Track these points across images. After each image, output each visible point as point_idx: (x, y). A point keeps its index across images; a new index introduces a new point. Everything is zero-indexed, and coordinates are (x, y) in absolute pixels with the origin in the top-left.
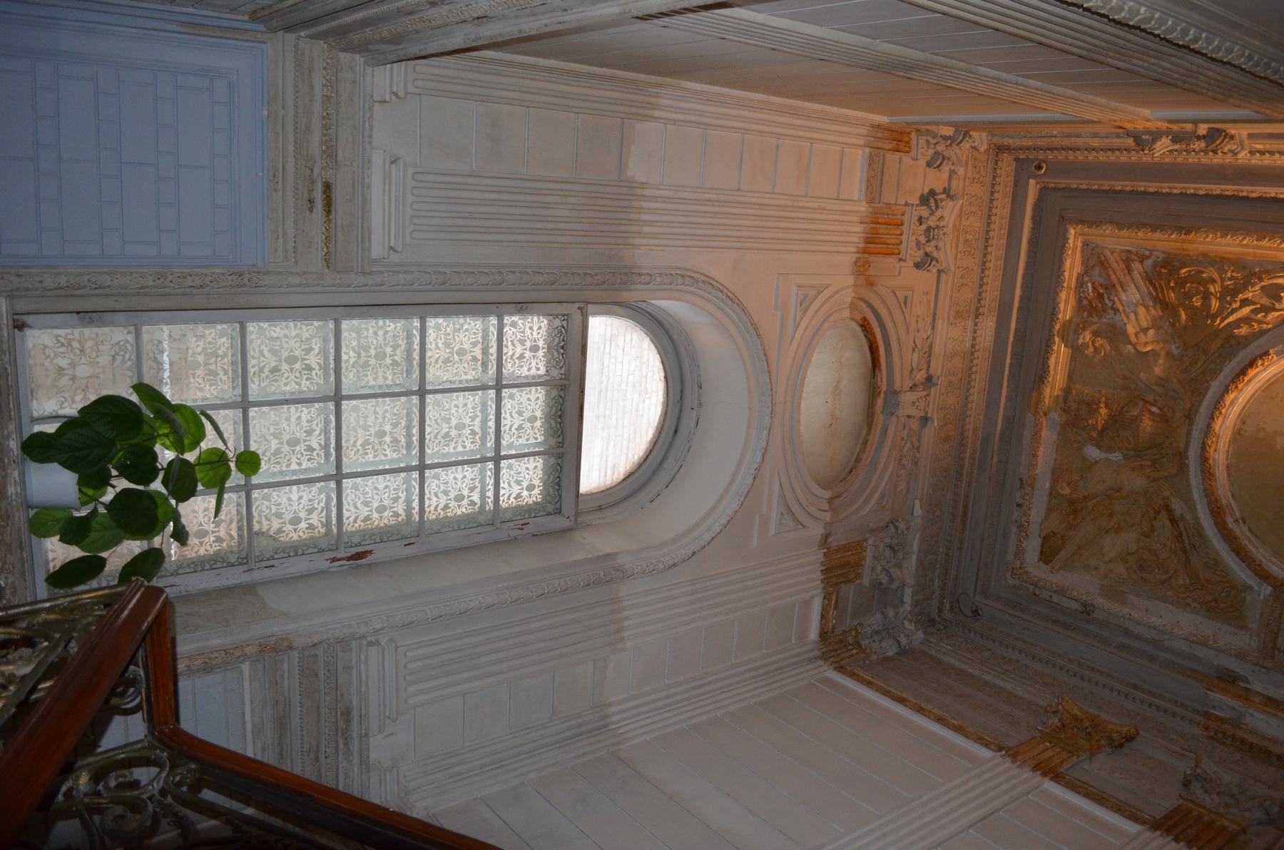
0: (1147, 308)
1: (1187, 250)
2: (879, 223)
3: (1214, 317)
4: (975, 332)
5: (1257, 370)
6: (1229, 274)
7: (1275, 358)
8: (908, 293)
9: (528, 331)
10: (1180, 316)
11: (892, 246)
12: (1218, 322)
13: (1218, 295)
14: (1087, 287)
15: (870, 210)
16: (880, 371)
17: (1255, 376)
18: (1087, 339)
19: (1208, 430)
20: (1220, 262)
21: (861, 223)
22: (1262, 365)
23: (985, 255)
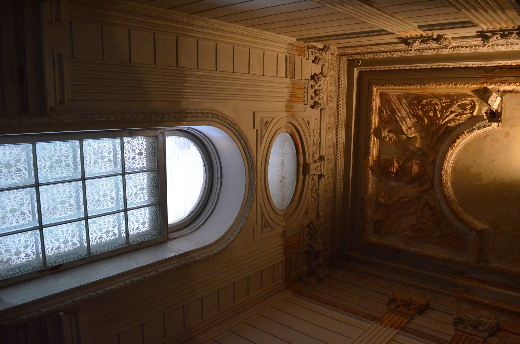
0: (410, 119)
1: (425, 92)
2: (295, 88)
3: (439, 120)
4: (337, 135)
5: (460, 140)
6: (444, 101)
7: (467, 134)
8: (309, 119)
10: (424, 121)
11: (301, 98)
12: (441, 121)
13: (440, 110)
14: (384, 112)
15: (291, 82)
17: (459, 143)
18: (386, 134)
19: (441, 168)
20: (439, 97)
21: (287, 88)
22: (462, 138)
23: (338, 102)
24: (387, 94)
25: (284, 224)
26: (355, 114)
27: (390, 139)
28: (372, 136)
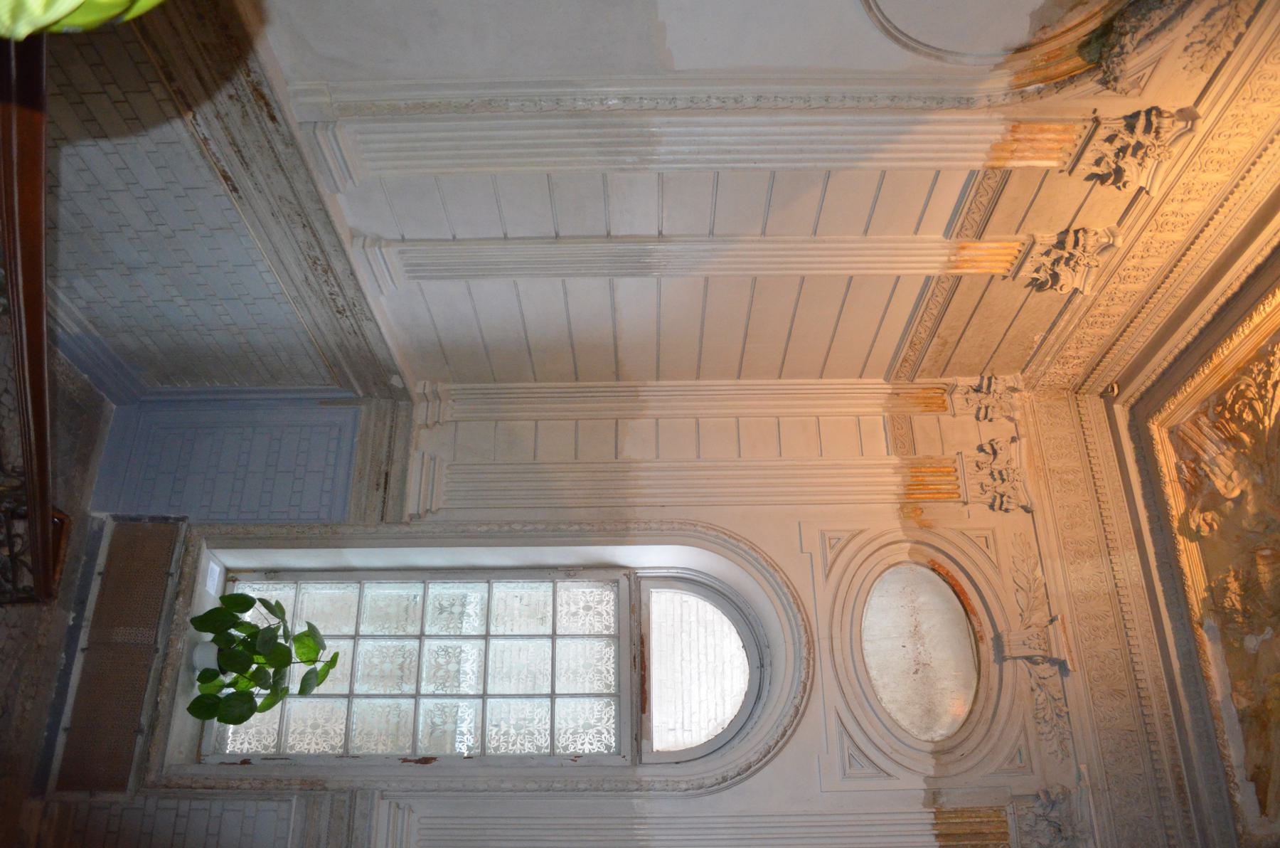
13: (1257, 396)
16: (975, 614)
24: (1177, 427)
25: (931, 772)
26: (1147, 506)
27: (1211, 526)
28: (1180, 538)
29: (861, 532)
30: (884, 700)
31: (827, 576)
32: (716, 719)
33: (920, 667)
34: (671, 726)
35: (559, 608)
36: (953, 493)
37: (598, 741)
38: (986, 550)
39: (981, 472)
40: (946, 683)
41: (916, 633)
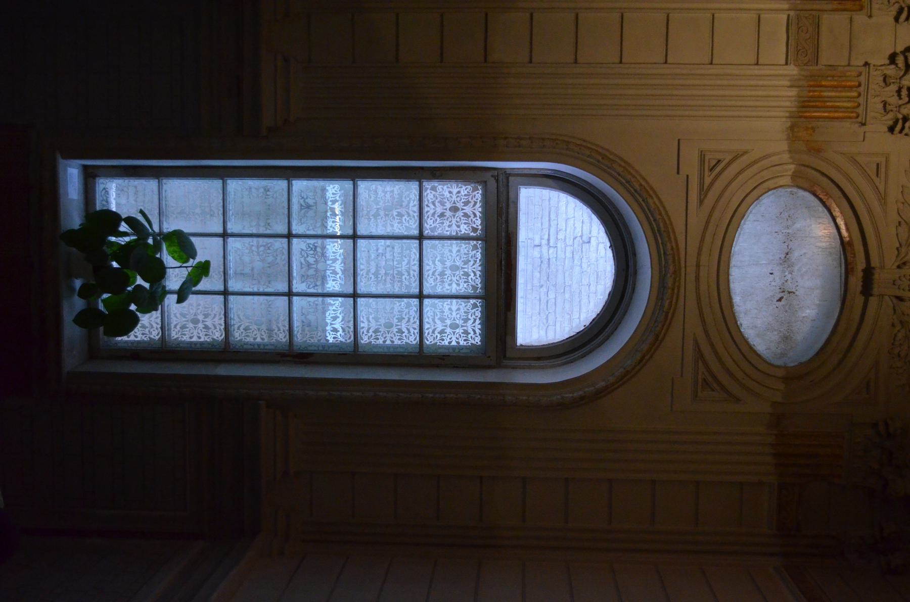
9: (447, 194)
29: (745, 153)
30: (744, 326)
31: (701, 202)
32: (581, 236)
33: (785, 295)
34: (537, 242)
35: (426, 209)
36: (852, 112)
37: (465, 282)
38: (874, 177)
39: (888, 89)
40: (808, 311)
41: (786, 260)
